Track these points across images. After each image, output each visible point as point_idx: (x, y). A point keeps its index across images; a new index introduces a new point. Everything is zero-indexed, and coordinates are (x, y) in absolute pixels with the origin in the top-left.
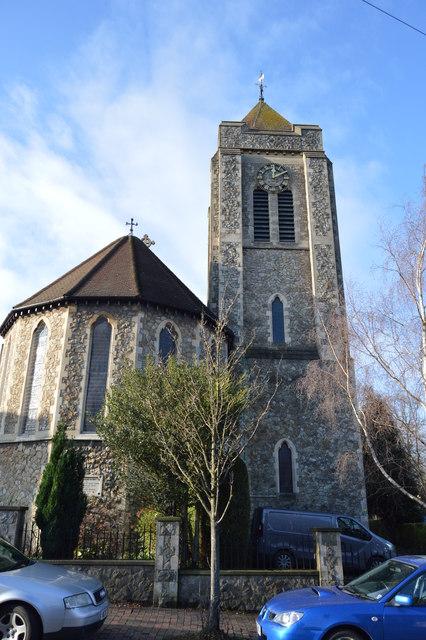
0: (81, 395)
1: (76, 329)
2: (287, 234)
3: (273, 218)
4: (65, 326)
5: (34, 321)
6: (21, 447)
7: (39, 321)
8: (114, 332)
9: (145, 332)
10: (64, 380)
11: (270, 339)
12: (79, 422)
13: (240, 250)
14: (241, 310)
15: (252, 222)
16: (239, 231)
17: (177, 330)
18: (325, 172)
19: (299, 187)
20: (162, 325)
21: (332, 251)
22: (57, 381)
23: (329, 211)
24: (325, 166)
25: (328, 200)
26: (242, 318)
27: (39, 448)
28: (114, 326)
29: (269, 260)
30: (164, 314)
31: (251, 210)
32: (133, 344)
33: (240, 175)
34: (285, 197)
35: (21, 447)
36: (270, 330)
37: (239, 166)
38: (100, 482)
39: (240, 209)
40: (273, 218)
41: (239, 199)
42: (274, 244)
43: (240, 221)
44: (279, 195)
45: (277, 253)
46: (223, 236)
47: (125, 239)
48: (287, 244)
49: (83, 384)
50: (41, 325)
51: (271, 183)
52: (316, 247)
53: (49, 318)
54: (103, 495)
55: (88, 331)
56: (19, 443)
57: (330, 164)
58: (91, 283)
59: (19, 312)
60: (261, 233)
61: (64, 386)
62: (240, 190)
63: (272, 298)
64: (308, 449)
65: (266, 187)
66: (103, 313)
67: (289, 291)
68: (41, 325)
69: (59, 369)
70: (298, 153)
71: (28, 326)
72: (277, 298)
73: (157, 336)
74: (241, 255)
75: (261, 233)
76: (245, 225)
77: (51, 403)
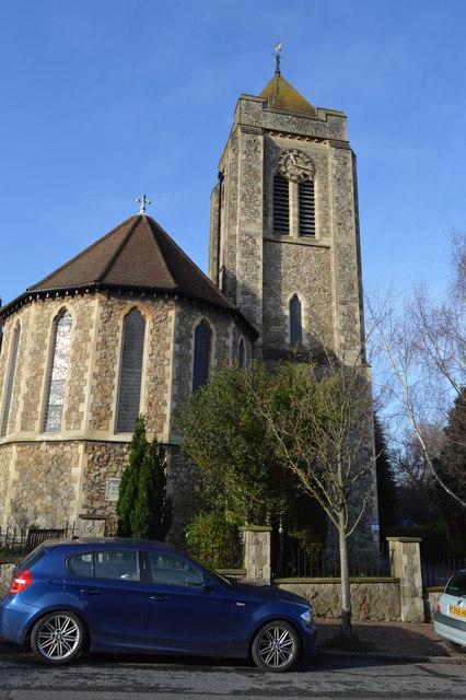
0: (115, 393)
1: (107, 318)
2: (306, 228)
3: (293, 210)
4: (95, 316)
5: (54, 307)
6: (44, 446)
8: (149, 326)
9: (183, 329)
10: (95, 376)
11: (288, 340)
12: (112, 423)
13: (260, 242)
14: (260, 307)
15: (271, 212)
16: (260, 220)
17: (212, 327)
18: (350, 165)
19: (321, 179)
20: (197, 322)
21: (354, 250)
22: (87, 376)
23: (352, 208)
24: (350, 159)
25: (351, 196)
26: (261, 316)
27: (67, 448)
28: (148, 320)
29: (289, 255)
30: (200, 309)
31: (270, 198)
32: (170, 340)
33: (261, 158)
34: (305, 187)
35: (44, 446)
36: (288, 331)
37: (261, 148)
39: (261, 196)
40: (293, 210)
41: (260, 185)
43: (261, 209)
44: (300, 185)
46: (243, 224)
47: (140, 218)
48: (306, 239)
49: (116, 381)
50: (63, 312)
51: (292, 169)
52: (338, 246)
53: (73, 306)
55: (120, 323)
56: (41, 442)
57: (354, 156)
58: (116, 269)
59: (34, 296)
60: (280, 225)
61: (95, 382)
62: (261, 175)
63: (290, 296)
65: (288, 175)
66: (136, 303)
68: (63, 312)
69: (89, 363)
70: (321, 140)
71: (46, 311)
72: (295, 296)
73: (193, 332)
74: (261, 247)
76: (265, 215)
77: (82, 400)
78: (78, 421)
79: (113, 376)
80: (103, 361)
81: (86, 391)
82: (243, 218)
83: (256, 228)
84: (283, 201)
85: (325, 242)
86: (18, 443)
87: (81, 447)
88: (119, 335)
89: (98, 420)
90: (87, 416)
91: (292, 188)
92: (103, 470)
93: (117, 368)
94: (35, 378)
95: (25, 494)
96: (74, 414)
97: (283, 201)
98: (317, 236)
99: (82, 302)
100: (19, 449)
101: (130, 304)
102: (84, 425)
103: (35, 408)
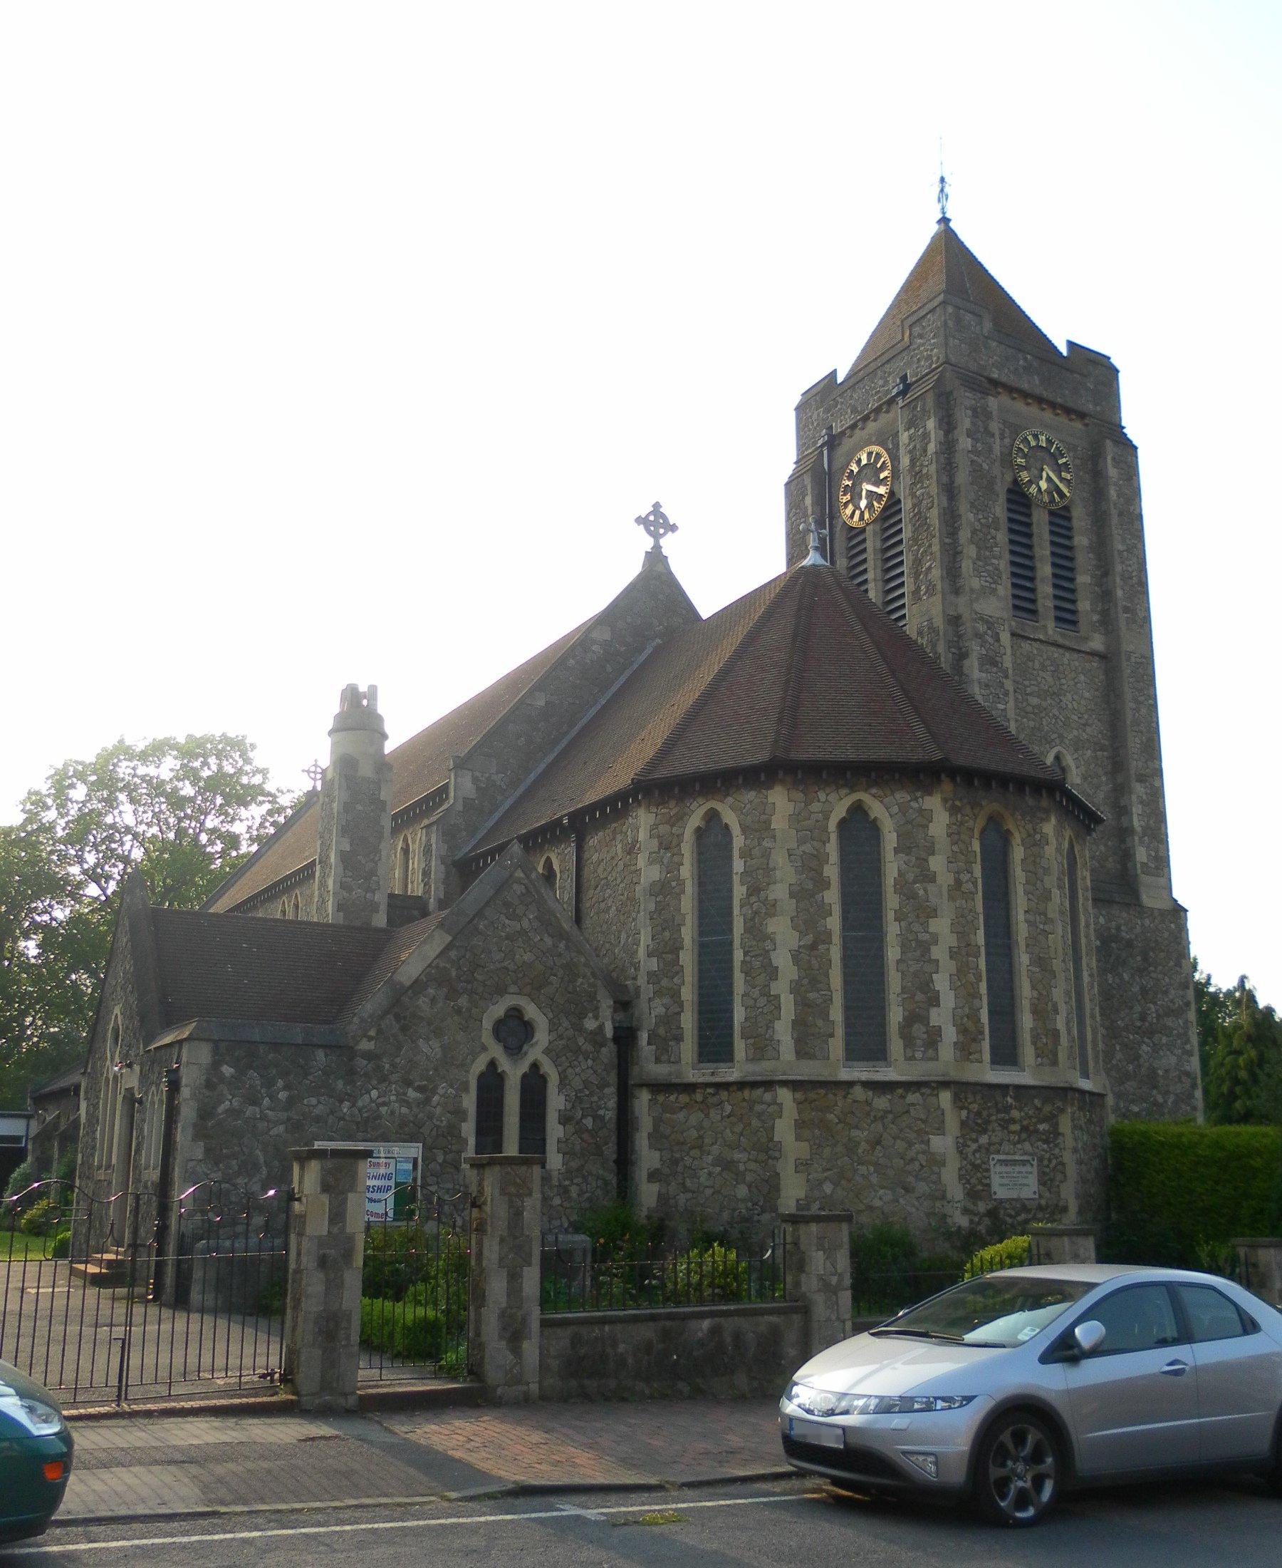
4: (940, 823)
6: (858, 1092)
7: (848, 802)
10: (953, 954)
16: (1005, 589)
27: (912, 1097)
34: (1061, 517)
35: (858, 1092)
38: (1035, 1170)
40: (1045, 570)
42: (1050, 632)
45: (1056, 653)
54: (1040, 1196)
56: (851, 1084)
64: (1130, 1086)
67: (1077, 746)
69: (942, 926)
71: (816, 807)
75: (1024, 605)
78: (934, 1037)
79: (977, 956)
80: (962, 929)
81: (941, 982)
82: (975, 583)
83: (997, 605)
84: (1067, 558)
85: (1097, 643)
86: (795, 1085)
87: (945, 1097)
88: (977, 870)
89: (966, 1049)
90: (950, 1034)
91: (1040, 520)
92: (984, 1140)
93: (980, 938)
94: (813, 947)
95: (828, 1188)
96: (918, 1030)
97: (1067, 558)
98: (1083, 626)
99: (902, 796)
100: (799, 1095)
101: (991, 805)
102: (947, 1051)
103: (825, 1014)
